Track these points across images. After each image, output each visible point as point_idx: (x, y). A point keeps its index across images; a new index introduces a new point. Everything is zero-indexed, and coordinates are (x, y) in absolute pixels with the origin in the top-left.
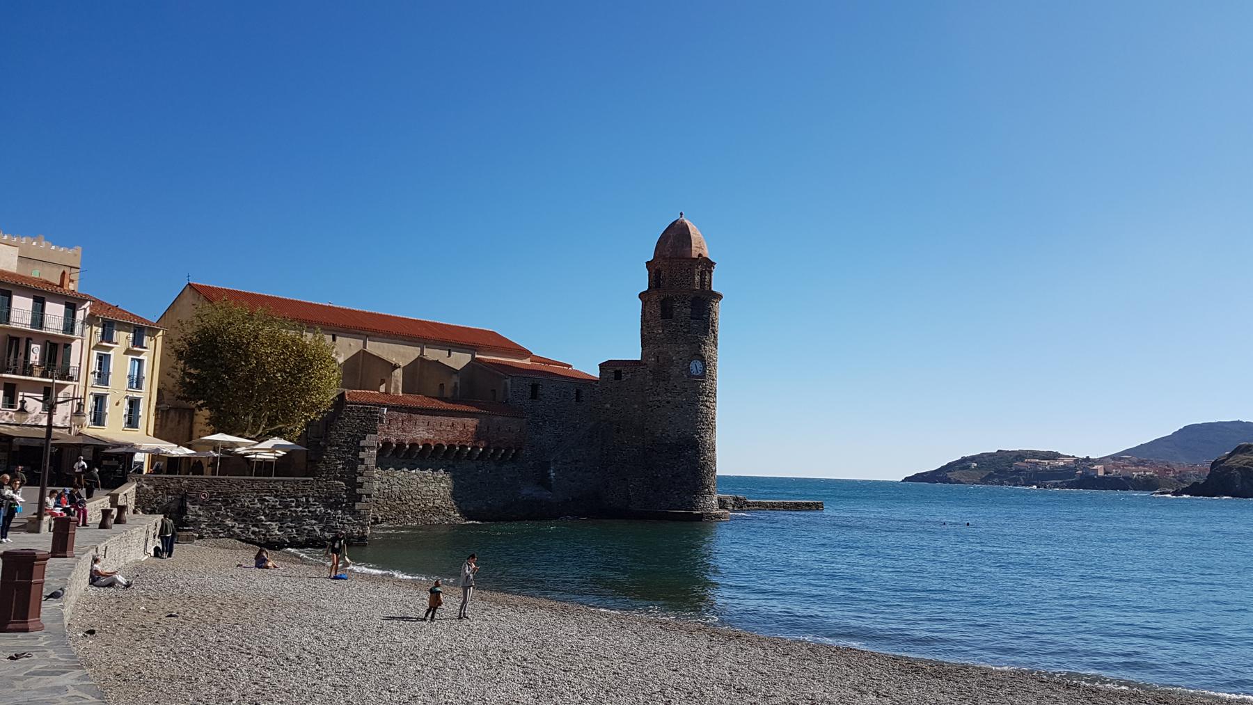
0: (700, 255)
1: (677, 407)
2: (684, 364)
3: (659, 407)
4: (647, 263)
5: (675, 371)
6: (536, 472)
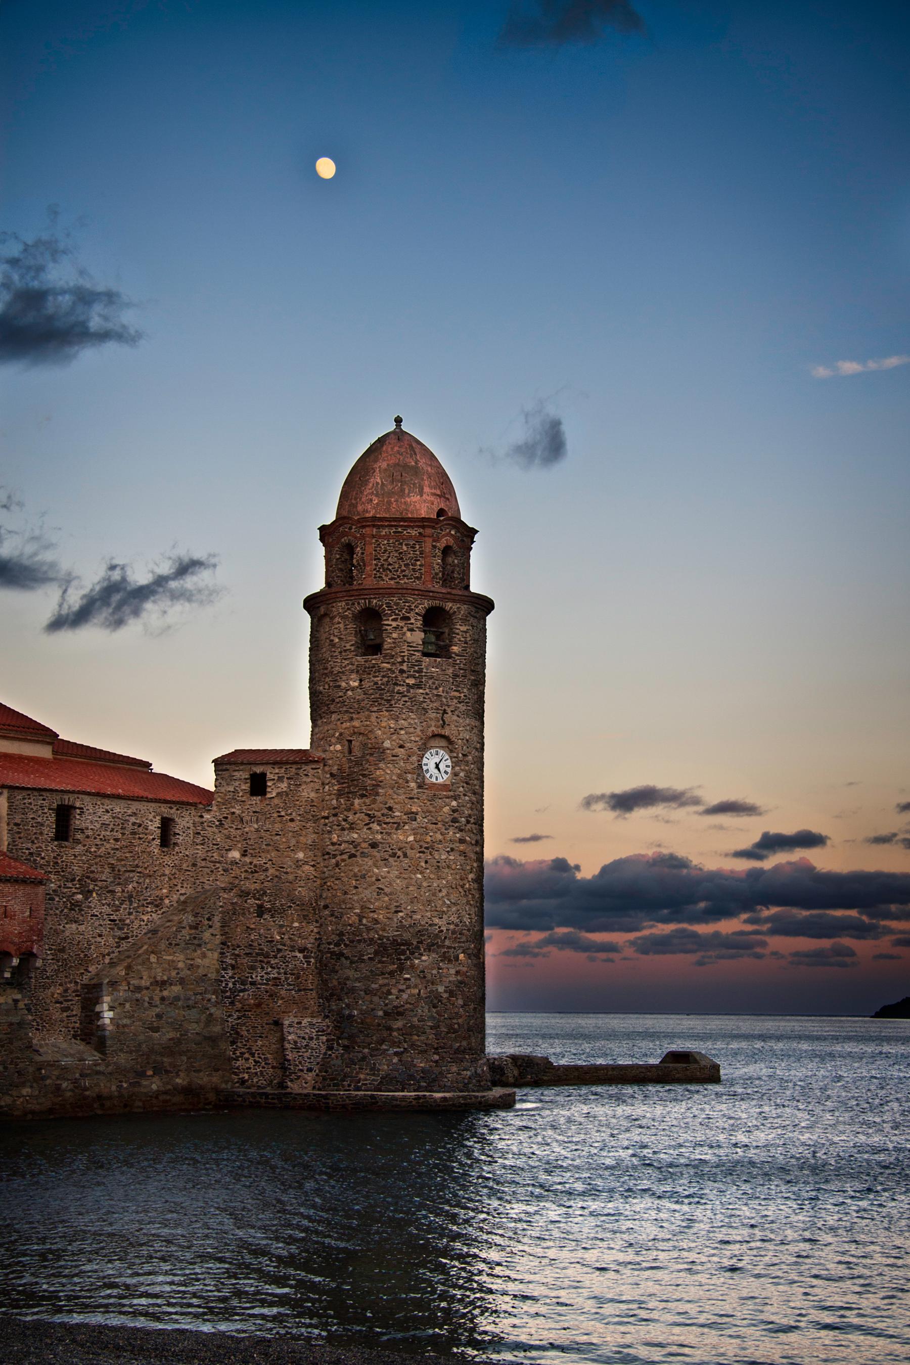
0: (441, 512)
3: (352, 856)
4: (323, 529)
5: (386, 772)
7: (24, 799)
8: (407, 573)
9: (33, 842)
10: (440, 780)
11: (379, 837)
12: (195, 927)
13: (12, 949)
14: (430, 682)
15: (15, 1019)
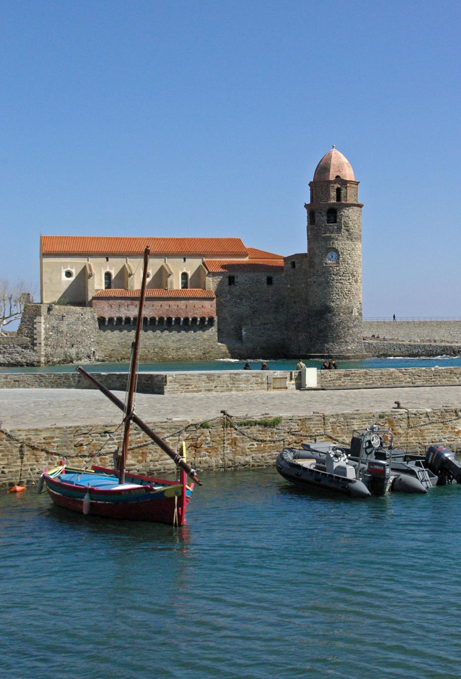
0: (338, 177)
2: (322, 255)
3: (311, 285)
6: (236, 331)
11: (315, 280)
12: (277, 307)
13: (205, 316)
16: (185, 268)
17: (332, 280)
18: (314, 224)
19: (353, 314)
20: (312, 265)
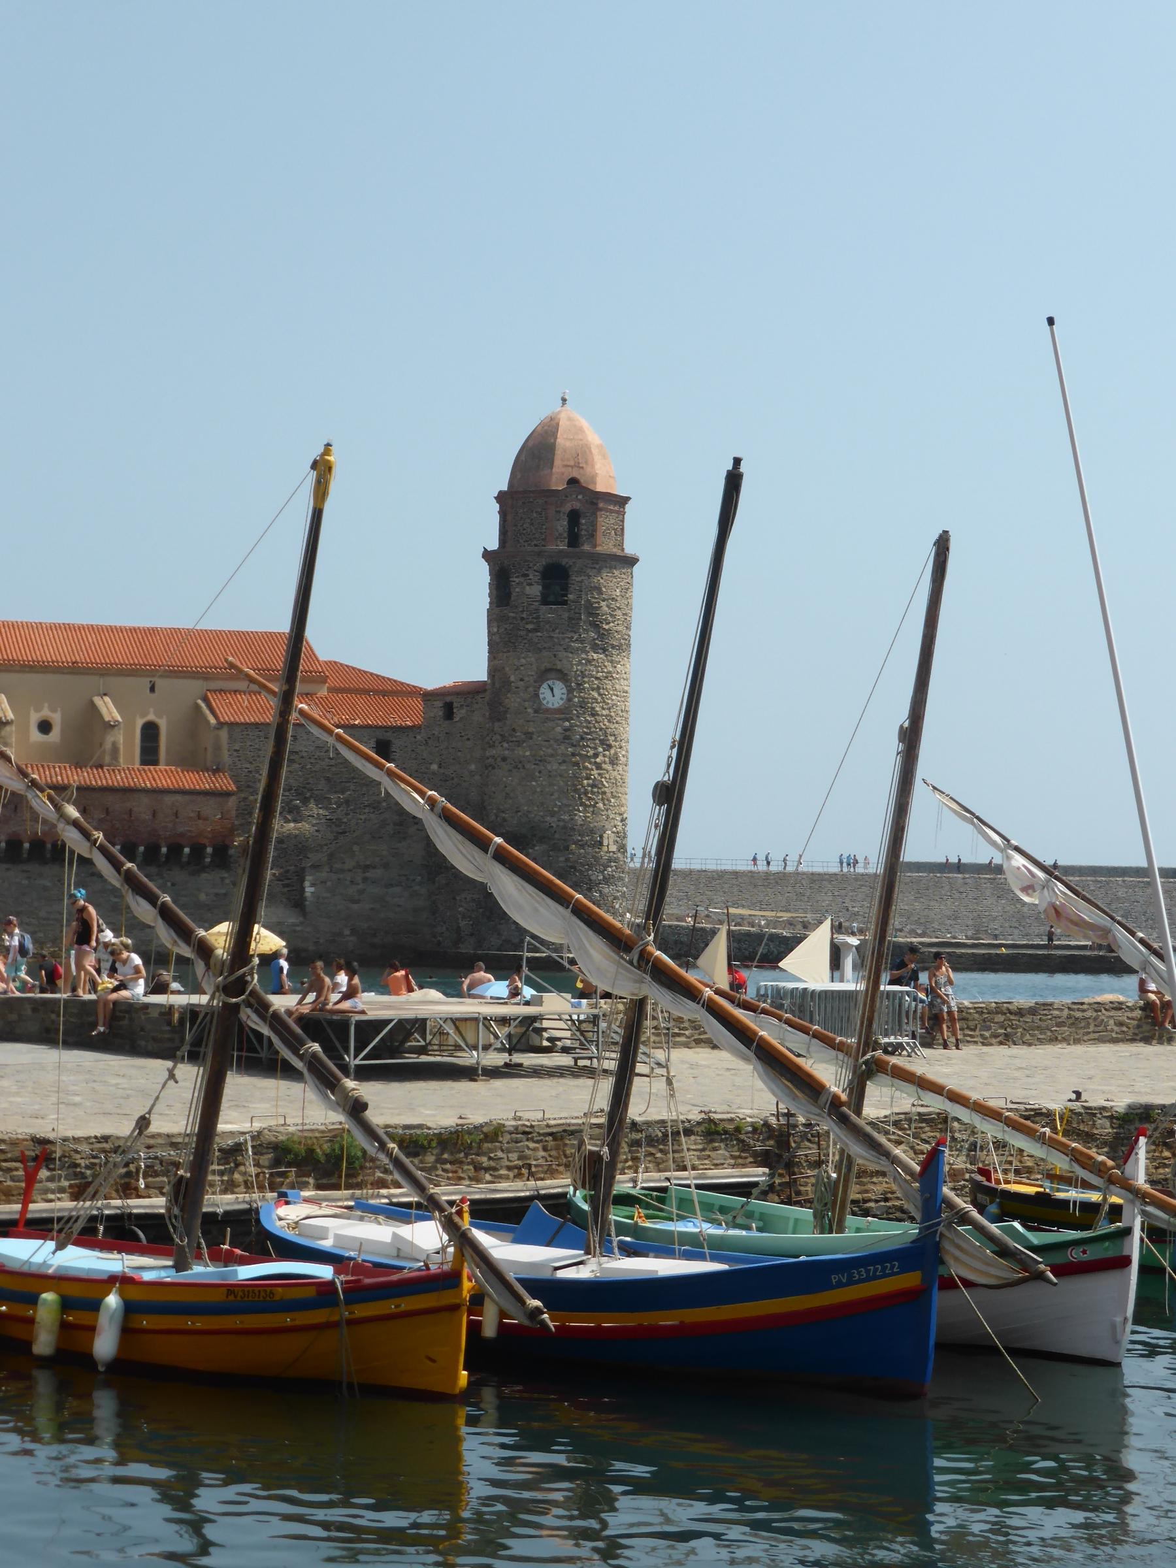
1: (516, 767)
3: (494, 768)
5: (512, 701)
6: (287, 886)
7: (242, 731)
8: (537, 536)
9: (251, 763)
10: (556, 706)
12: (400, 824)
13: (206, 841)
14: (547, 626)
15: (223, 891)
16: (151, 710)
17: (552, 756)
18: (507, 605)
19: (605, 849)
20: (497, 711)
